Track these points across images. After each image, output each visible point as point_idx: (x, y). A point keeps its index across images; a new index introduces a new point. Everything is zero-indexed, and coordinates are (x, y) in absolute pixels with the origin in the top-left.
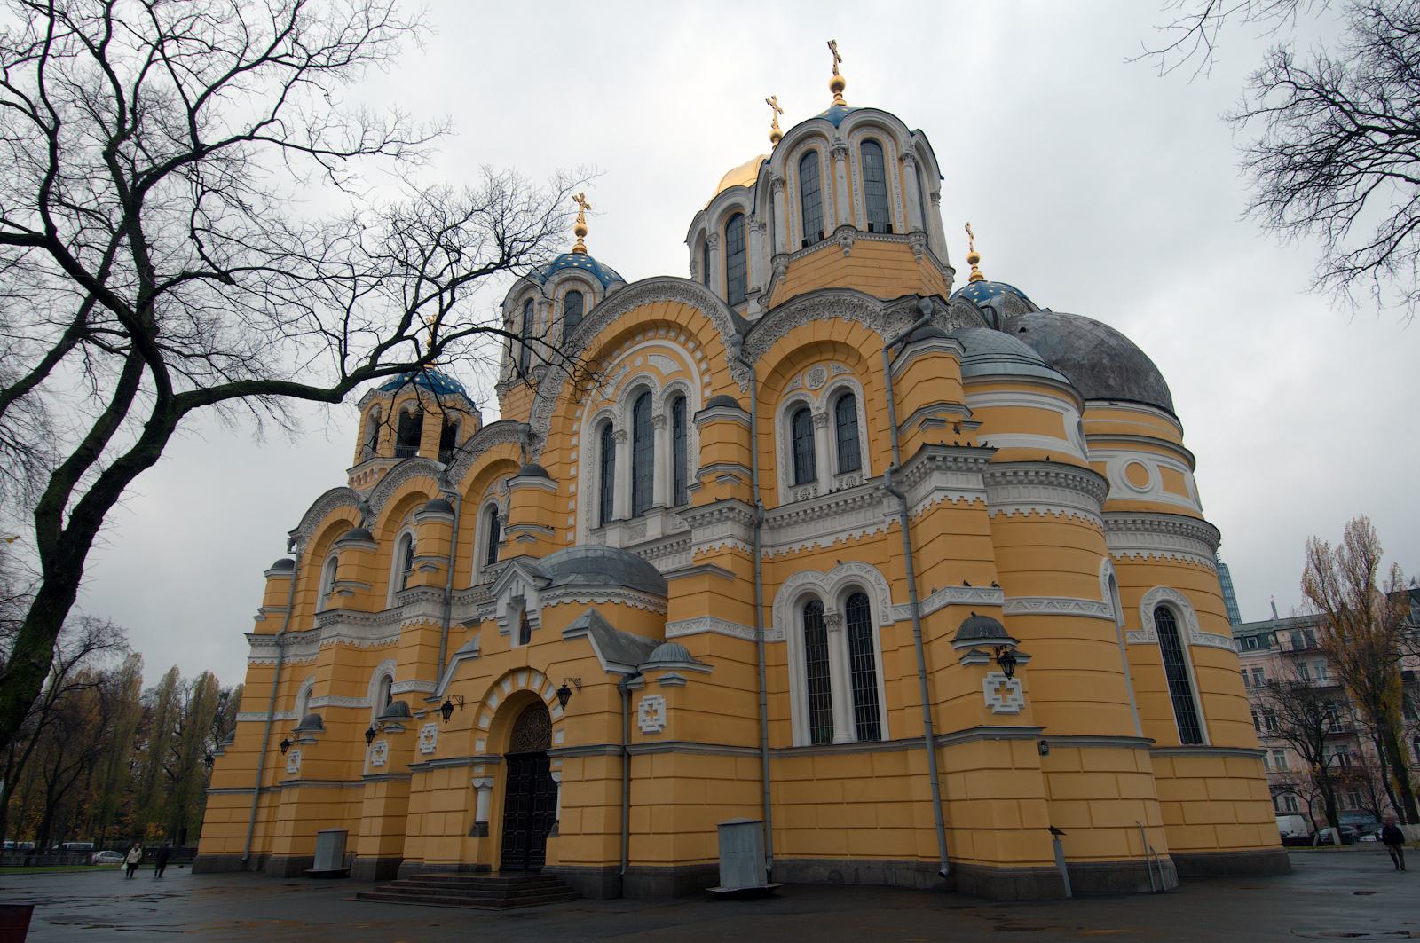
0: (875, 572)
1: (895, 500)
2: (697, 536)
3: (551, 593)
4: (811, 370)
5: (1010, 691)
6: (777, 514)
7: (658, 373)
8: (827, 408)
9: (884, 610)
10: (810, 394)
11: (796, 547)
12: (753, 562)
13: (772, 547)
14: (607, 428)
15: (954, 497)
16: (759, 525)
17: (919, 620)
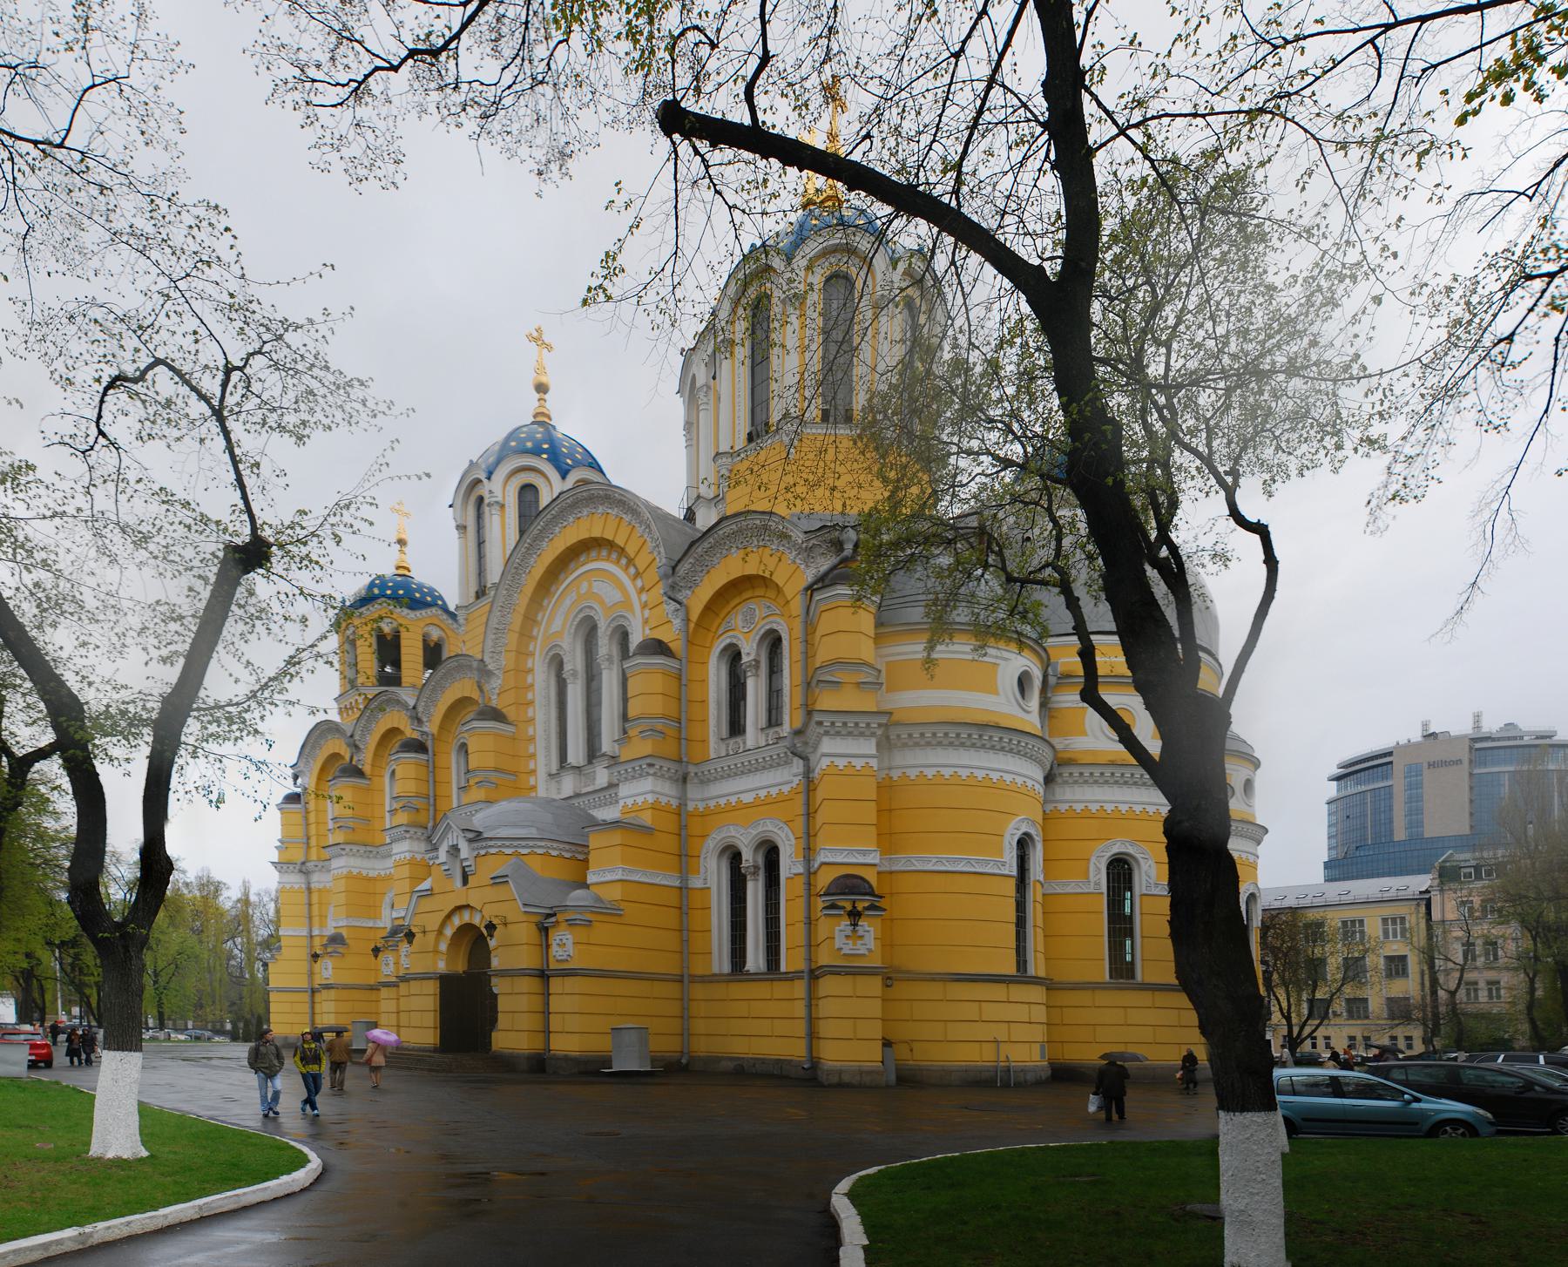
0: (786, 828)
1: (801, 761)
2: (624, 790)
3: (480, 844)
4: (743, 608)
5: (861, 937)
6: (705, 768)
7: (601, 602)
8: (758, 654)
9: (789, 865)
10: (741, 636)
11: (722, 801)
12: (679, 815)
13: (703, 800)
14: (557, 663)
15: (841, 763)
16: (684, 779)
17: (810, 874)
